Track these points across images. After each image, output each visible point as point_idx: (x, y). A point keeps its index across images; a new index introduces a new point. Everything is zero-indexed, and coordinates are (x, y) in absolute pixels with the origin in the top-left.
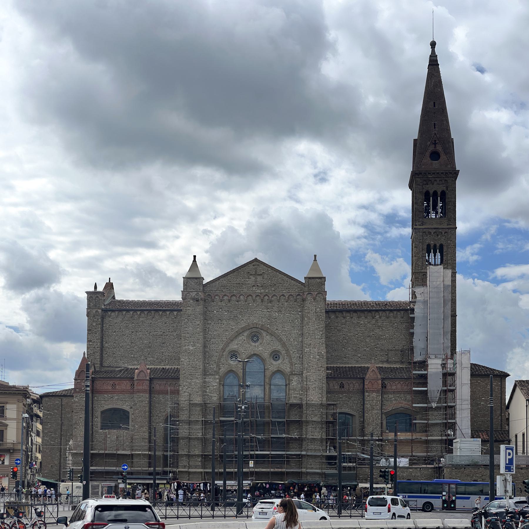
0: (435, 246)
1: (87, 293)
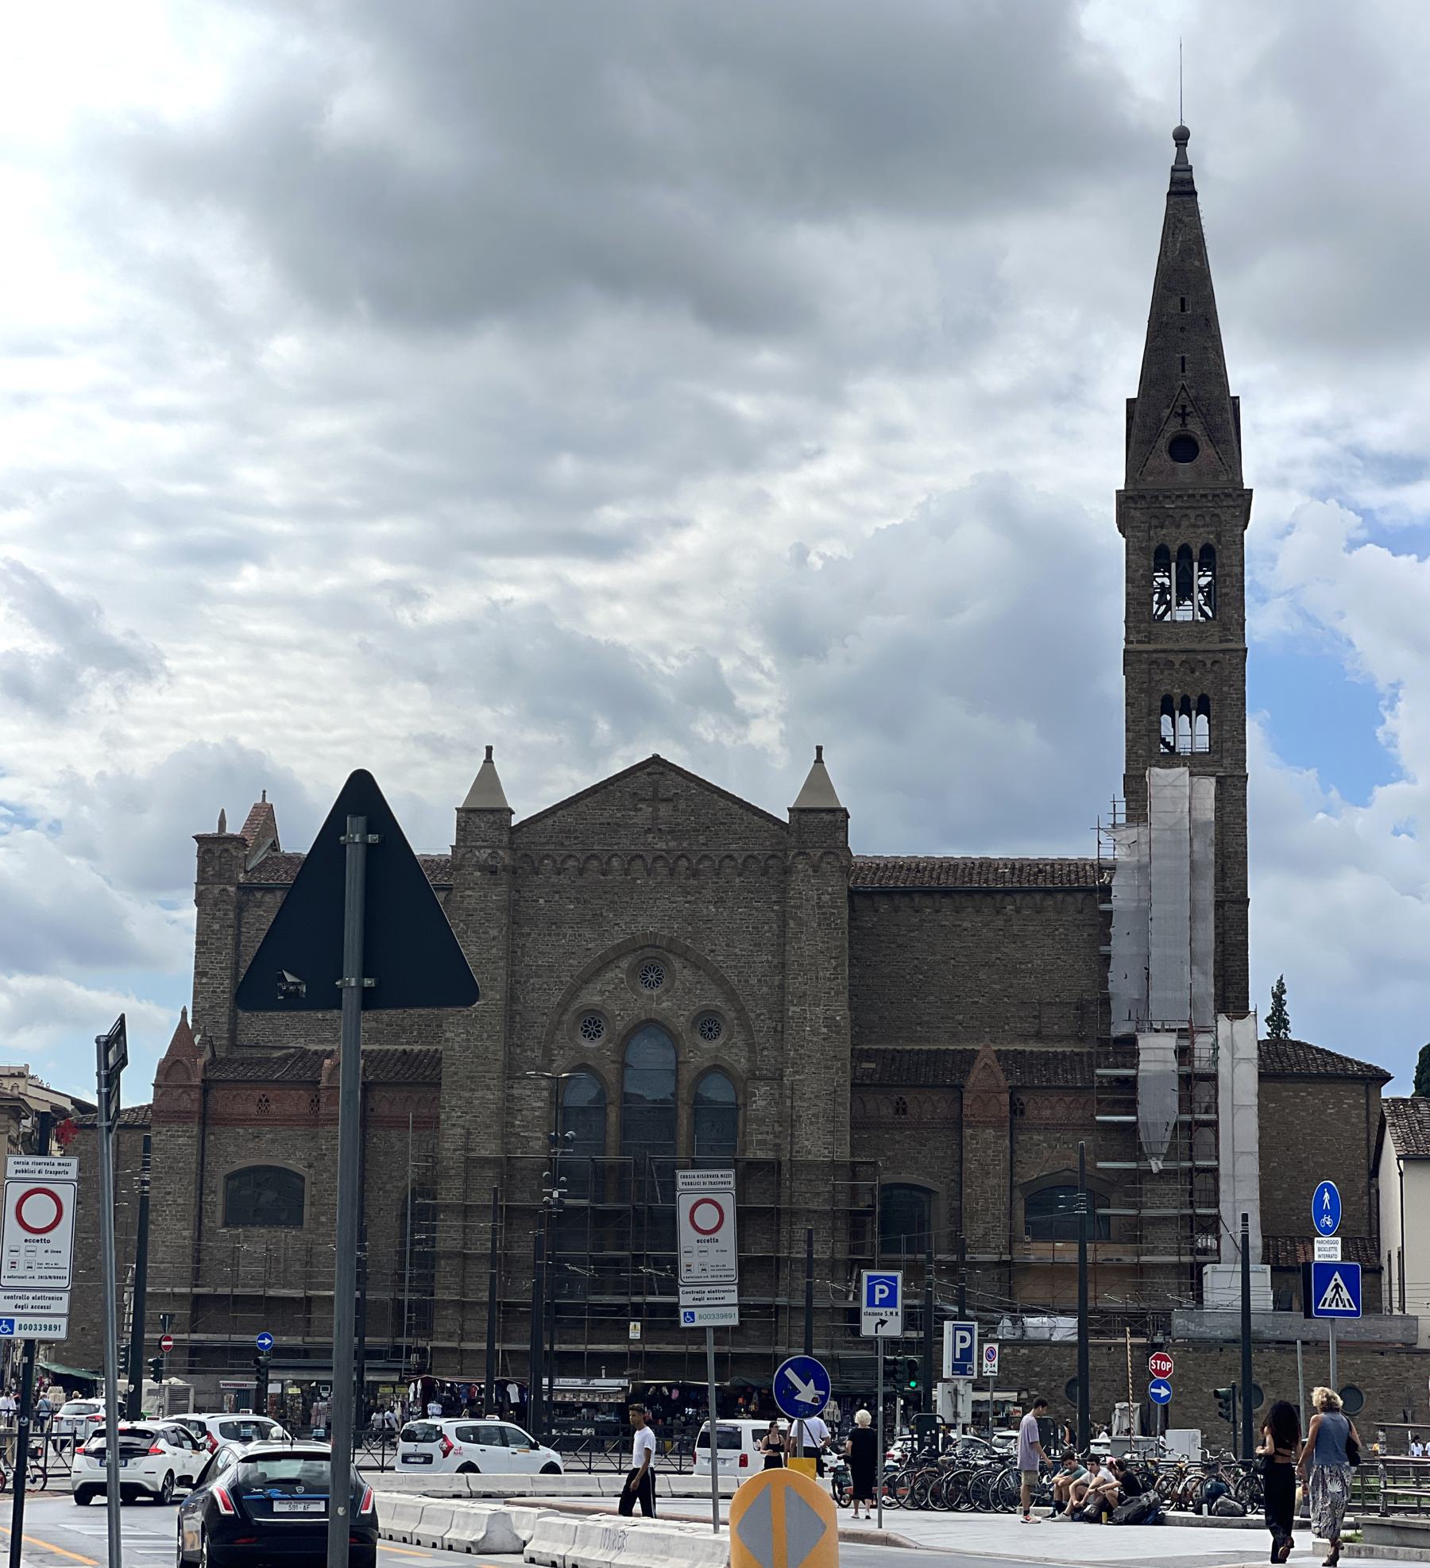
0: (1185, 700)
1: (197, 838)
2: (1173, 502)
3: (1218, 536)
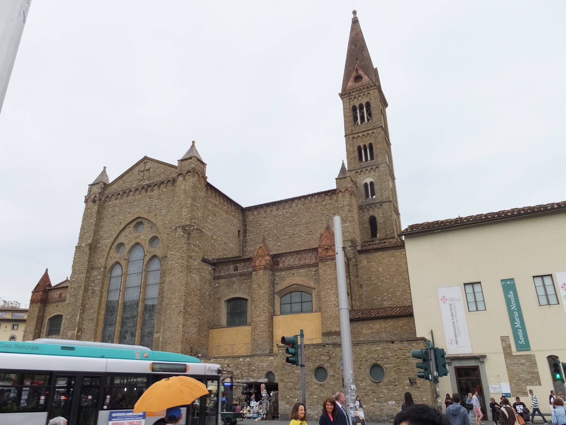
2: (355, 93)
3: (370, 98)
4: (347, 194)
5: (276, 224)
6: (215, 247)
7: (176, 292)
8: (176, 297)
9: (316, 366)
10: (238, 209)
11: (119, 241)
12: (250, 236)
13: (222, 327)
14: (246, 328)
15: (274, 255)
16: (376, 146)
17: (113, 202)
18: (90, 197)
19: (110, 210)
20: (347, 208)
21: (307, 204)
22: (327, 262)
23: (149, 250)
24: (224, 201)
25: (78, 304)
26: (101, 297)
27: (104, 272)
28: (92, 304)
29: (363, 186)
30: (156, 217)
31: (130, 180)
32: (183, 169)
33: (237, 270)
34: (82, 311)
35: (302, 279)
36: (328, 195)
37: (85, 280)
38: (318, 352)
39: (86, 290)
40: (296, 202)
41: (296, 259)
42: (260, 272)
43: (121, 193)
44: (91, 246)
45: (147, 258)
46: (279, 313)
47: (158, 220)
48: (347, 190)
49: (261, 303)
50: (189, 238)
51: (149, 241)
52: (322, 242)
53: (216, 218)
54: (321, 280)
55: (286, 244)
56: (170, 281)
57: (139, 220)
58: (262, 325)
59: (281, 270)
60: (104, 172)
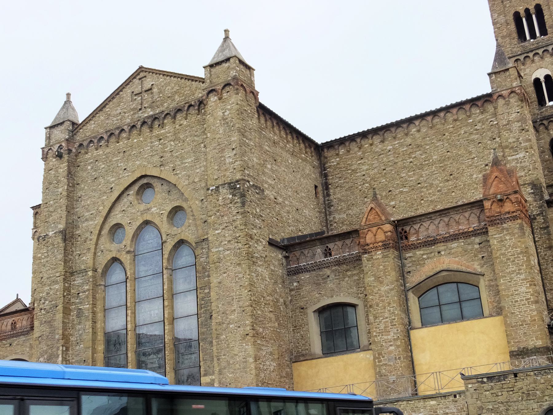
4: (514, 100)
5: (384, 168)
6: (282, 217)
7: (233, 300)
8: (235, 310)
9: (545, 407)
10: (310, 148)
11: (112, 221)
12: (336, 194)
13: (311, 357)
14: (362, 355)
15: (398, 221)
16: (549, 8)
17: (93, 153)
18: (51, 149)
19: (89, 168)
20: (516, 126)
21: (438, 126)
22: (504, 225)
23: (169, 232)
24: (287, 134)
25: (57, 337)
26: (94, 322)
27: (94, 277)
28: (81, 335)
29: (532, 85)
30: (175, 172)
31: (118, 112)
32: (214, 81)
33: (331, 255)
34: (64, 349)
35: (457, 259)
36: (478, 106)
37: (63, 294)
38: (546, 381)
39: (67, 311)
40: (417, 124)
41: (440, 225)
42: (376, 254)
43: (106, 137)
44: (65, 233)
45: (168, 247)
46: (420, 325)
47: (179, 177)
48: (512, 92)
49: (385, 308)
50: (243, 204)
51: (168, 217)
52: (490, 189)
53: (278, 166)
54: (497, 258)
55: (407, 202)
56: (220, 283)
57: (145, 181)
58: (392, 348)
59: (415, 247)
60: (68, 102)
